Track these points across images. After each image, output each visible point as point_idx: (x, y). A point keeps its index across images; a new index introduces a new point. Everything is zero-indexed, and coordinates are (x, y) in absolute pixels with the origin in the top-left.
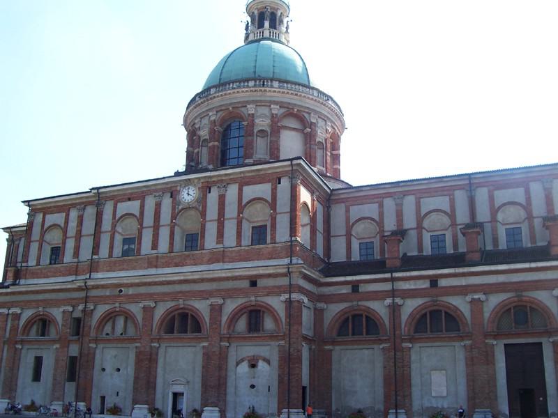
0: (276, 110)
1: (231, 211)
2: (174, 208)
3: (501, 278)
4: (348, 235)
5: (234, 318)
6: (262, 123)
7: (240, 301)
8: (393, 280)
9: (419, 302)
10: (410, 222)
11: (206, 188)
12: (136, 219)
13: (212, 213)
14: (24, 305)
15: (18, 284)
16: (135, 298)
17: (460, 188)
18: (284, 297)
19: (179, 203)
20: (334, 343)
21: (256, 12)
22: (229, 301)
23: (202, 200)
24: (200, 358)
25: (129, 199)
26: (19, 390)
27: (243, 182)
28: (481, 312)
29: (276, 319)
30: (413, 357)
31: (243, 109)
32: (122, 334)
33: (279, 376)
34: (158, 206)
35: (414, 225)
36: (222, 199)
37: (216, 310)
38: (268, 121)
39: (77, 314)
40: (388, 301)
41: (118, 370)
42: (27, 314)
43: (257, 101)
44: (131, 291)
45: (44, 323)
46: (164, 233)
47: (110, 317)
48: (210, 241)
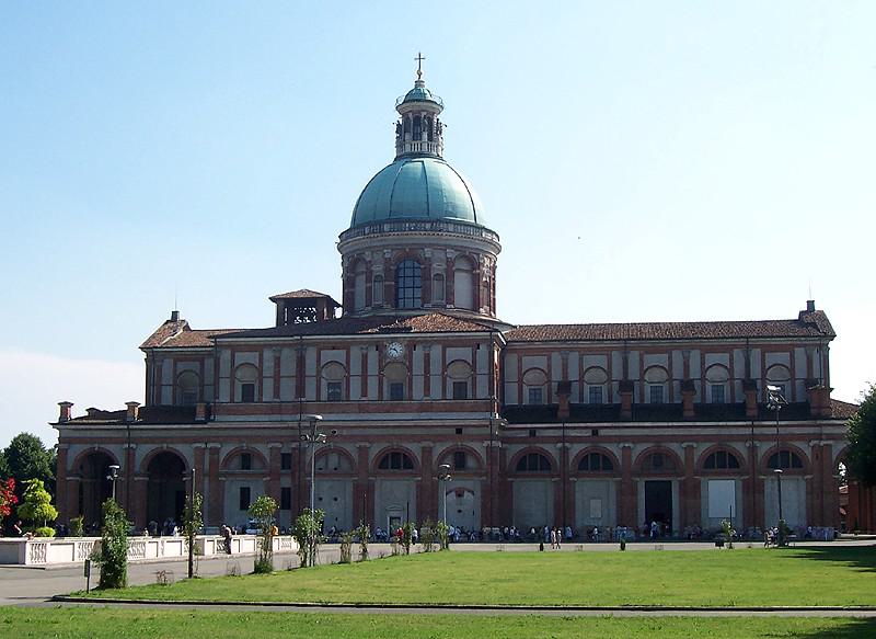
0: (451, 254)
1: (436, 368)
2: (380, 361)
3: (646, 432)
4: (520, 383)
6: (438, 267)
7: (449, 444)
9: (582, 446)
10: (573, 376)
11: (411, 345)
13: (418, 368)
14: (226, 440)
15: (213, 421)
16: (346, 438)
19: (386, 356)
20: (515, 476)
21: (410, 115)
22: (438, 444)
23: (409, 356)
24: (413, 491)
25: (334, 349)
28: (630, 456)
29: (478, 459)
30: (577, 489)
33: (482, 503)
34: (365, 357)
36: (427, 358)
37: (427, 452)
38: (445, 266)
40: (560, 445)
41: (336, 499)
43: (434, 245)
44: (345, 432)
45: (247, 459)
46: (373, 383)
48: (418, 393)
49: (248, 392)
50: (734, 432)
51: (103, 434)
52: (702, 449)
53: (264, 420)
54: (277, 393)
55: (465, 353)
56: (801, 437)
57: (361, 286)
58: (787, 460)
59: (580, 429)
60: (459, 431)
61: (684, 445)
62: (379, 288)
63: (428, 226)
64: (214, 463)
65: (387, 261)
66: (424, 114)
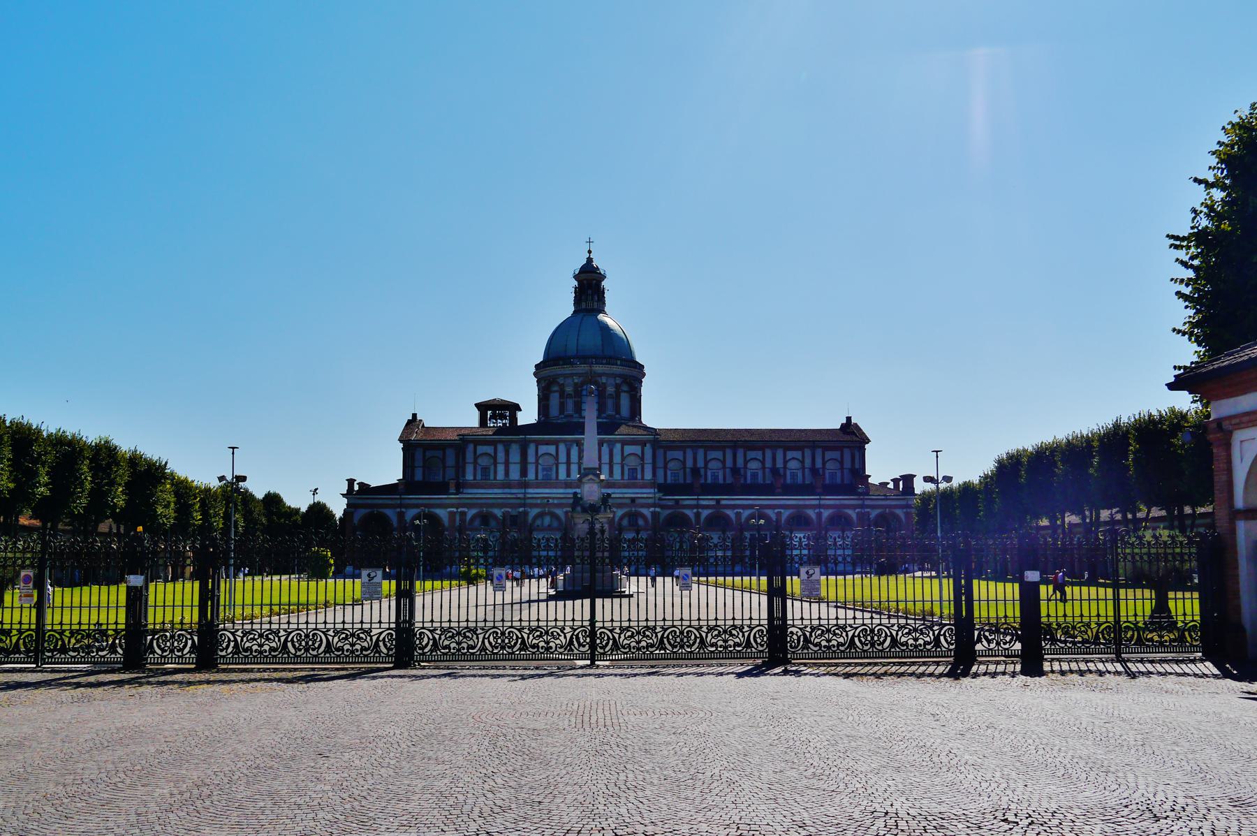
0: (618, 381)
1: (617, 459)
3: (750, 502)
4: (665, 468)
5: (622, 518)
6: (610, 390)
8: (698, 499)
9: (710, 511)
14: (470, 506)
15: (462, 493)
17: (729, 447)
18: (652, 509)
25: (547, 444)
27: (624, 443)
28: (740, 518)
32: (549, 526)
35: (702, 465)
38: (614, 389)
39: (514, 512)
40: (695, 510)
42: (471, 513)
44: (556, 501)
45: (485, 519)
46: (574, 468)
47: (541, 515)
49: (485, 470)
50: (807, 503)
52: (786, 514)
53: (496, 493)
54: (507, 473)
55: (637, 449)
56: (848, 507)
57: (555, 400)
58: (840, 521)
59: (708, 500)
60: (633, 500)
61: (776, 511)
62: (570, 404)
63: (605, 361)
64: (463, 520)
65: (576, 384)
66: (594, 282)
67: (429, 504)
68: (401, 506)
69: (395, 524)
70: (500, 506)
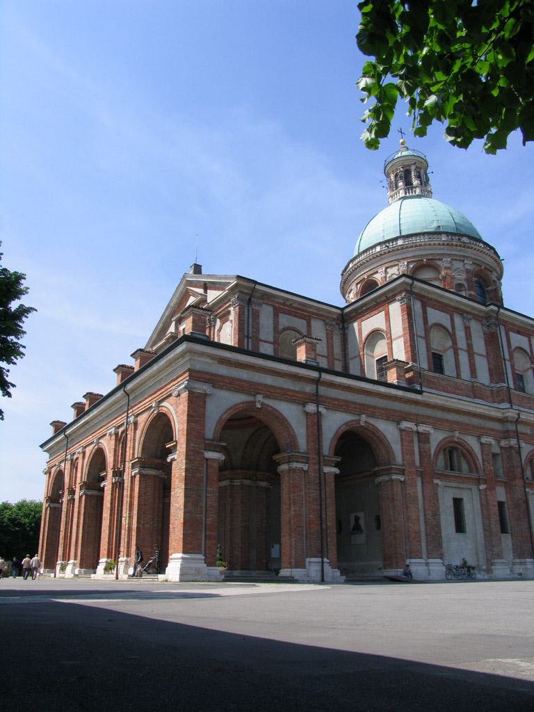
12: (528, 358)
26: (444, 545)
31: (489, 273)
51: (269, 380)
67: (369, 406)
68: (317, 399)
69: (302, 443)
70: (479, 433)
